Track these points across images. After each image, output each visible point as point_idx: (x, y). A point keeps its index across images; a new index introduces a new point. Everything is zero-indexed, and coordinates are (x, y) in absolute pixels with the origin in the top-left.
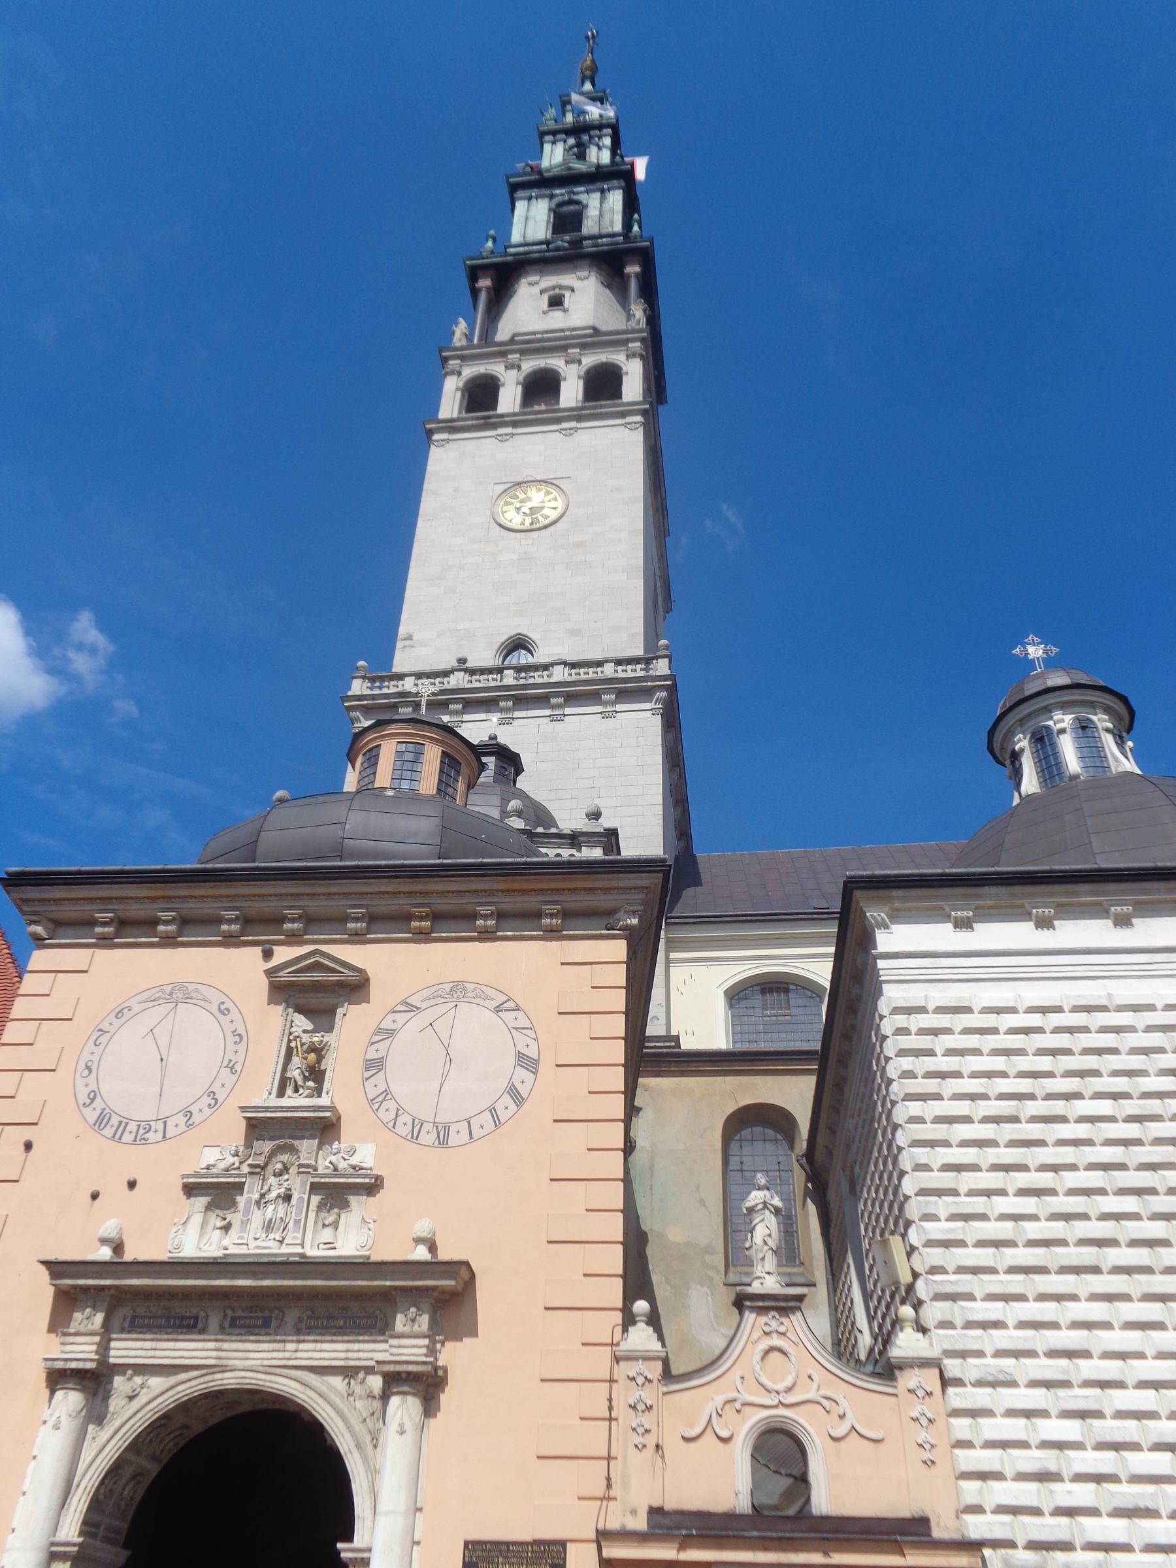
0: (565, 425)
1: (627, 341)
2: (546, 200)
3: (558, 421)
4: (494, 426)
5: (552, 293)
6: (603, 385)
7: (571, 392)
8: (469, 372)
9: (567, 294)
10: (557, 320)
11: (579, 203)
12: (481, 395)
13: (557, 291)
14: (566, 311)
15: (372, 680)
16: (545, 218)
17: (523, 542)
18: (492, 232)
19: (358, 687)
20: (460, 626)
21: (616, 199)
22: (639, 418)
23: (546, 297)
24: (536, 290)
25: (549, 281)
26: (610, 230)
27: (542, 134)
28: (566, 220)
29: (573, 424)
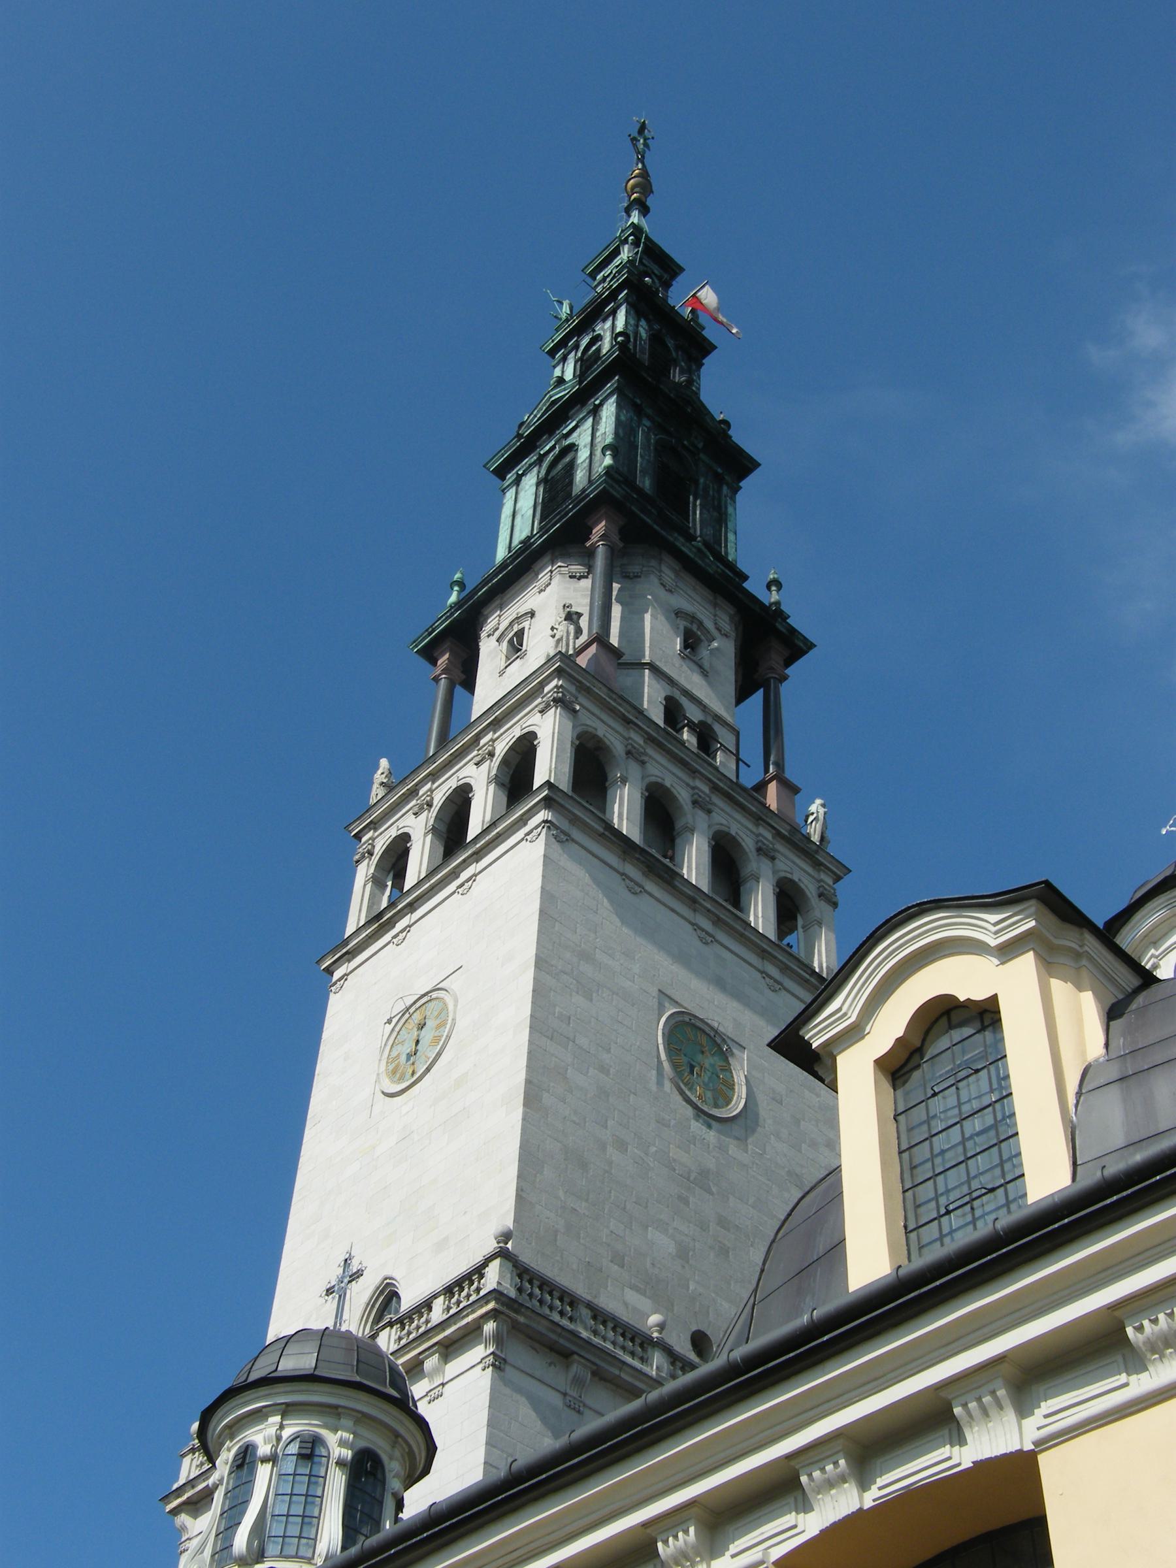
0: (464, 875)
9: (526, 624)
10: (519, 671)
13: (516, 628)
18: (457, 576)
23: (505, 644)
24: (494, 638)
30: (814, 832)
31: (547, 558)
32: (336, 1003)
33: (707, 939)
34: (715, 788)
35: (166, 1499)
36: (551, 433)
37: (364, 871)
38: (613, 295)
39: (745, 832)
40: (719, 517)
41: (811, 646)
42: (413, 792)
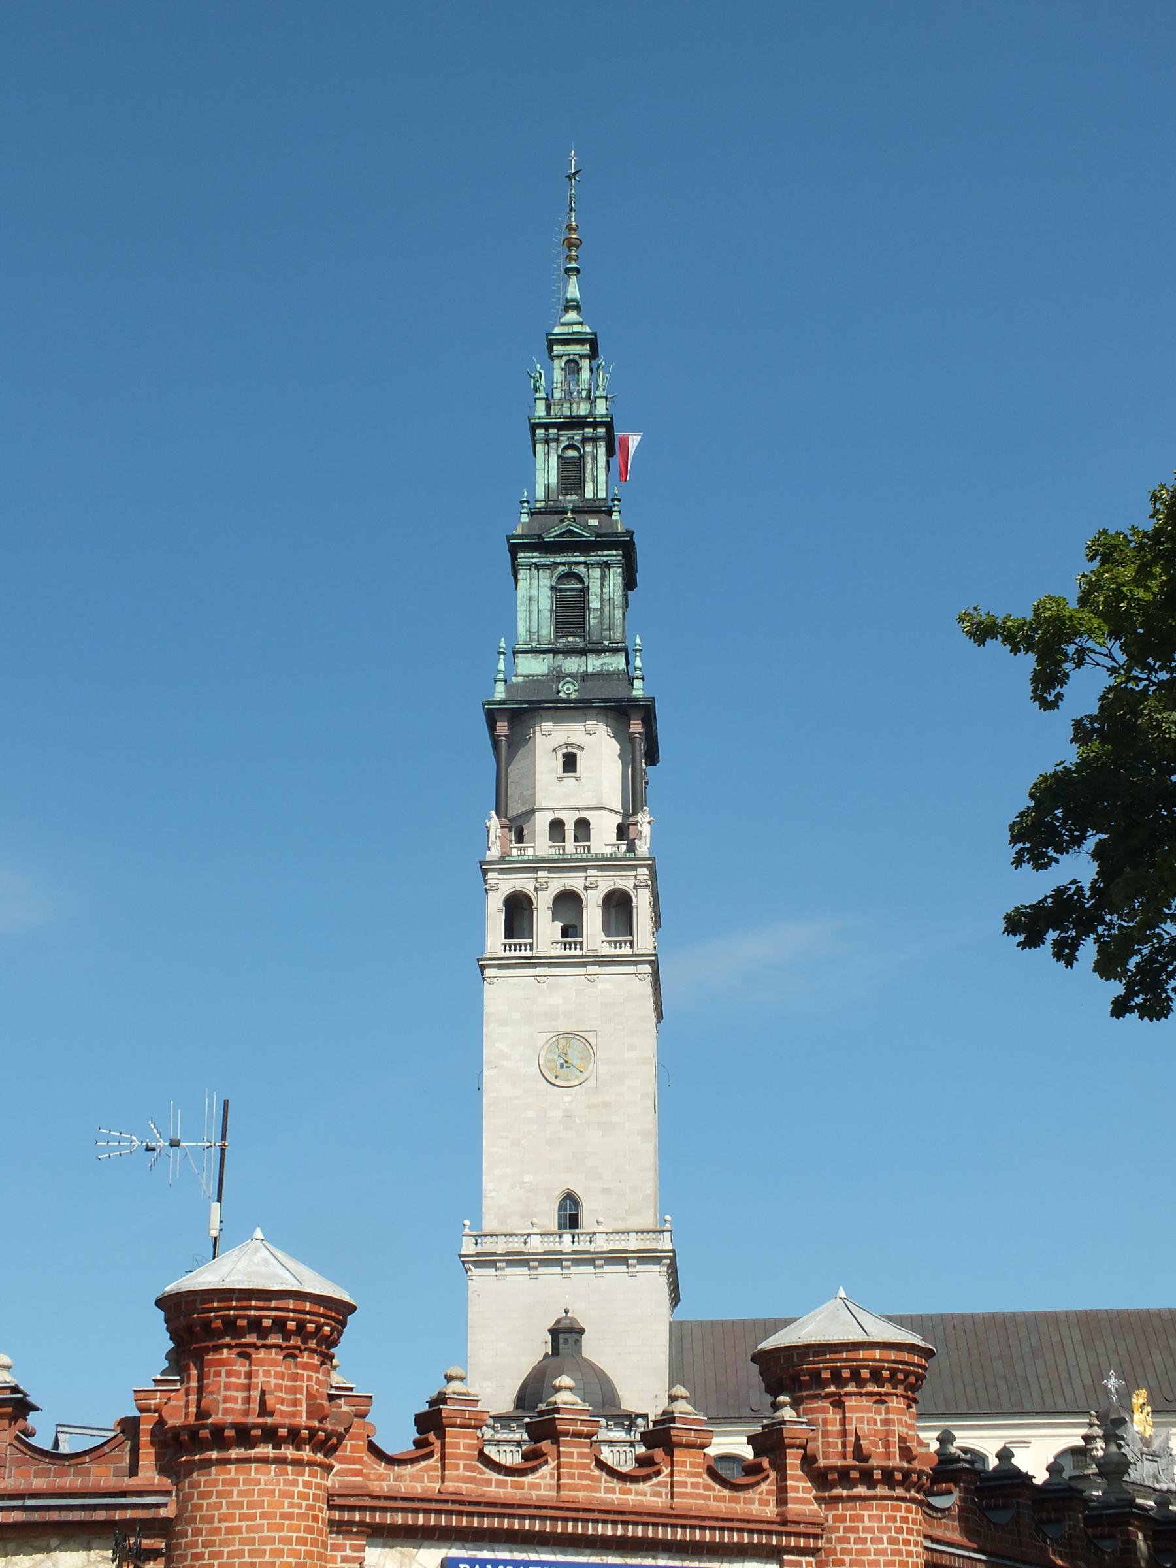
0: (591, 969)
1: (635, 867)
2: (548, 573)
4: (534, 966)
5: (565, 751)
11: (580, 579)
12: (518, 911)
13: (570, 750)
14: (578, 779)
16: (549, 607)
17: (566, 1099)
19: (468, 1247)
20: (527, 1178)
21: (615, 577)
23: (560, 754)
27: (534, 427)
31: (595, 711)
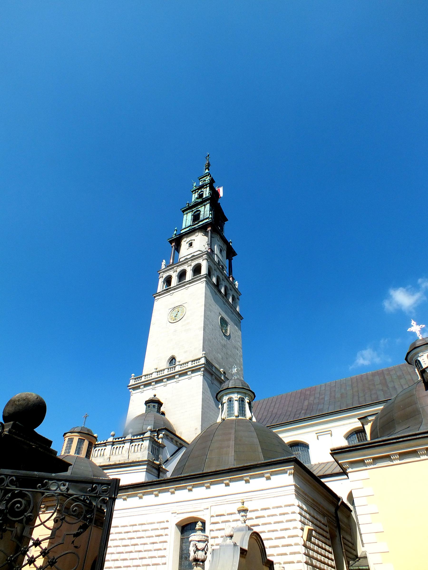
0: (186, 286)
3: (184, 286)
6: (197, 270)
7: (189, 275)
8: (165, 275)
10: (191, 250)
11: (199, 210)
13: (191, 242)
15: (135, 379)
18: (176, 228)
19: (132, 382)
22: (205, 279)
23: (188, 244)
25: (188, 239)
26: (206, 217)
28: (196, 218)
29: (188, 285)
30: (237, 287)
31: (198, 231)
32: (156, 303)
33: (224, 304)
34: (225, 277)
35: (128, 386)
36: (195, 207)
37: (161, 281)
38: (206, 185)
39: (228, 285)
40: (222, 229)
41: (237, 255)
42: (173, 268)
